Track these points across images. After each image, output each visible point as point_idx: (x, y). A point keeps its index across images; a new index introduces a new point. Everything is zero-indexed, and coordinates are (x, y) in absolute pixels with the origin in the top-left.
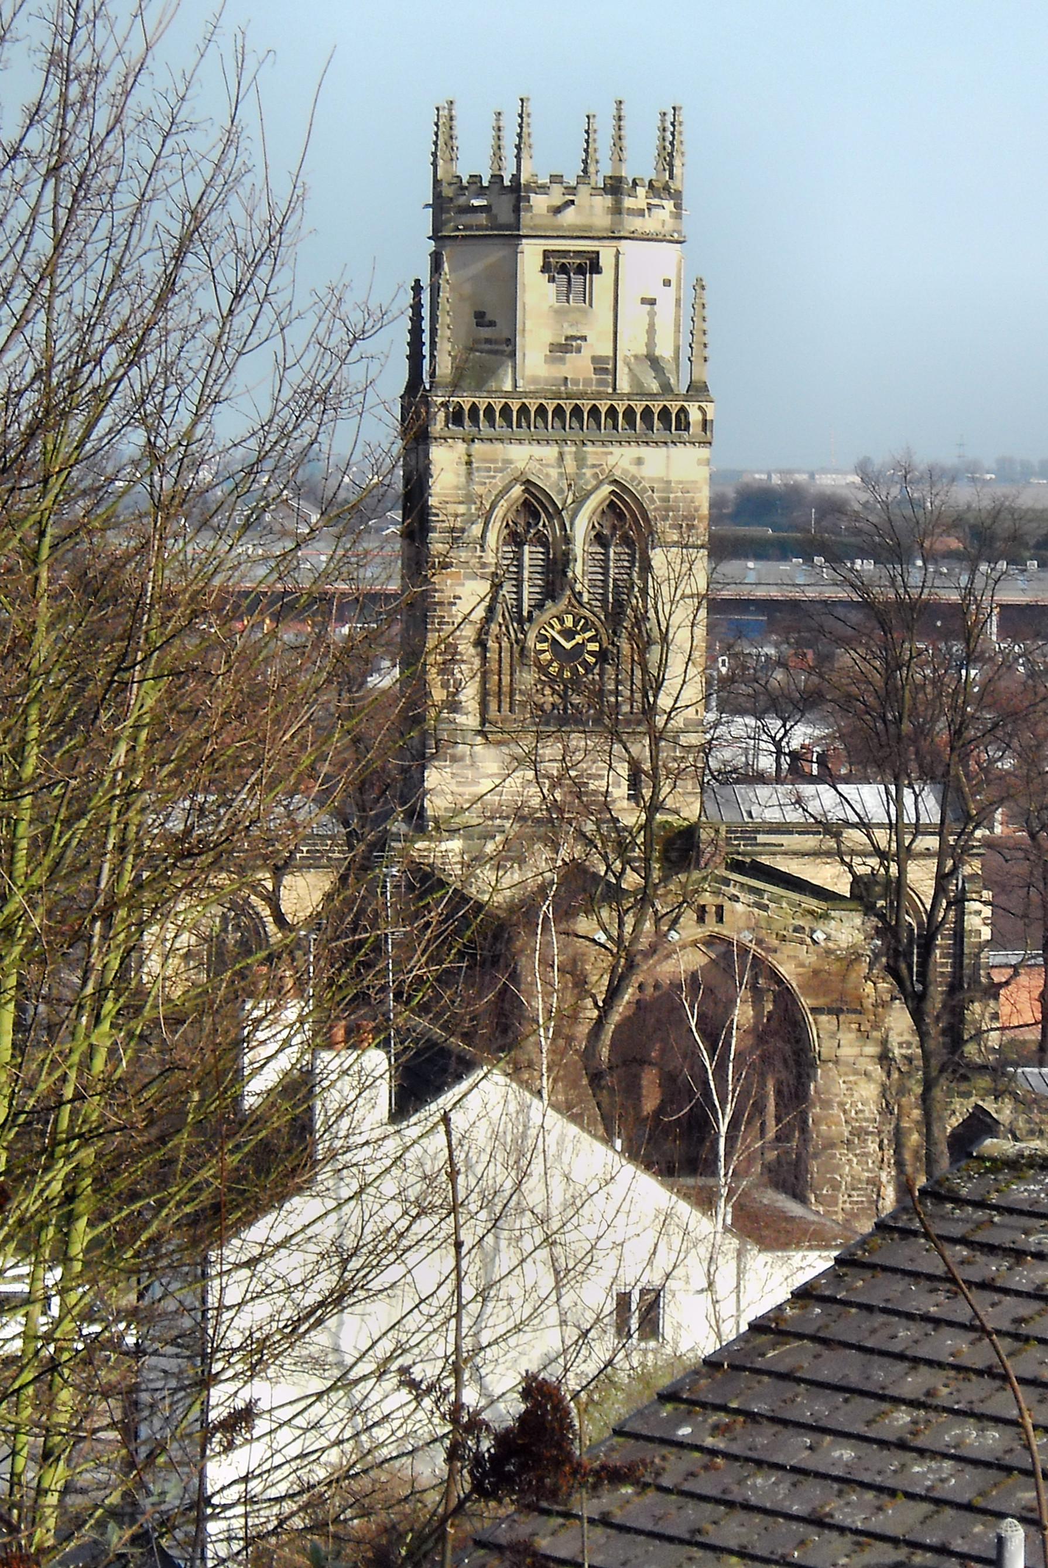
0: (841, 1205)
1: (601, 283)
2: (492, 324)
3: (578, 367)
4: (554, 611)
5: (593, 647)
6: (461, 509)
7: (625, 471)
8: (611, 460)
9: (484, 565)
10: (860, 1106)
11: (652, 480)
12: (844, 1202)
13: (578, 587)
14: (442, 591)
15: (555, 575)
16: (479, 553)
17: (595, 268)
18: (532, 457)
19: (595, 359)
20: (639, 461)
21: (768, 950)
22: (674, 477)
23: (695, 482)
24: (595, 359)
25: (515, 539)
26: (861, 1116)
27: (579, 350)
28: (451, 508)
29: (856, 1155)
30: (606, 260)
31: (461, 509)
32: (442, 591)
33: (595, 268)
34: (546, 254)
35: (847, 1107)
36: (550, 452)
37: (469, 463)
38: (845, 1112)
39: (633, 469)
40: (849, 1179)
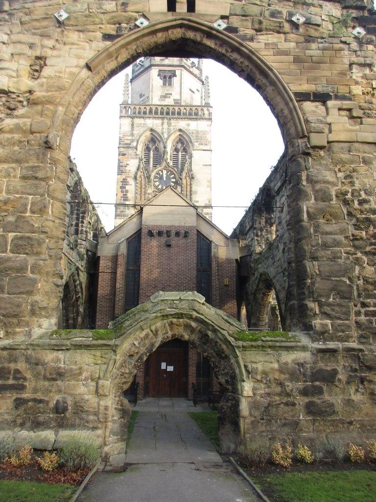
0: (353, 317)
1: (176, 80)
2: (144, 95)
3: (169, 101)
4: (160, 168)
5: (174, 180)
6: (130, 138)
7: (184, 128)
8: (179, 124)
9: (137, 155)
10: (363, 196)
11: (192, 130)
12: (358, 314)
13: (169, 161)
14: (122, 162)
15: (159, 159)
16: (135, 151)
17: (175, 75)
18: (151, 123)
19: (174, 100)
20: (188, 125)
21: (244, 38)
22: (200, 129)
23: (207, 131)
24: (174, 100)
25: (148, 149)
26: (366, 206)
27: (170, 97)
28: (126, 138)
29: (366, 253)
30: (178, 73)
31: (130, 138)
32: (122, 162)
33: (175, 75)
34: (160, 71)
35: (349, 196)
36: (159, 122)
37: (133, 125)
38: (346, 203)
39: (186, 127)
40: (361, 282)
